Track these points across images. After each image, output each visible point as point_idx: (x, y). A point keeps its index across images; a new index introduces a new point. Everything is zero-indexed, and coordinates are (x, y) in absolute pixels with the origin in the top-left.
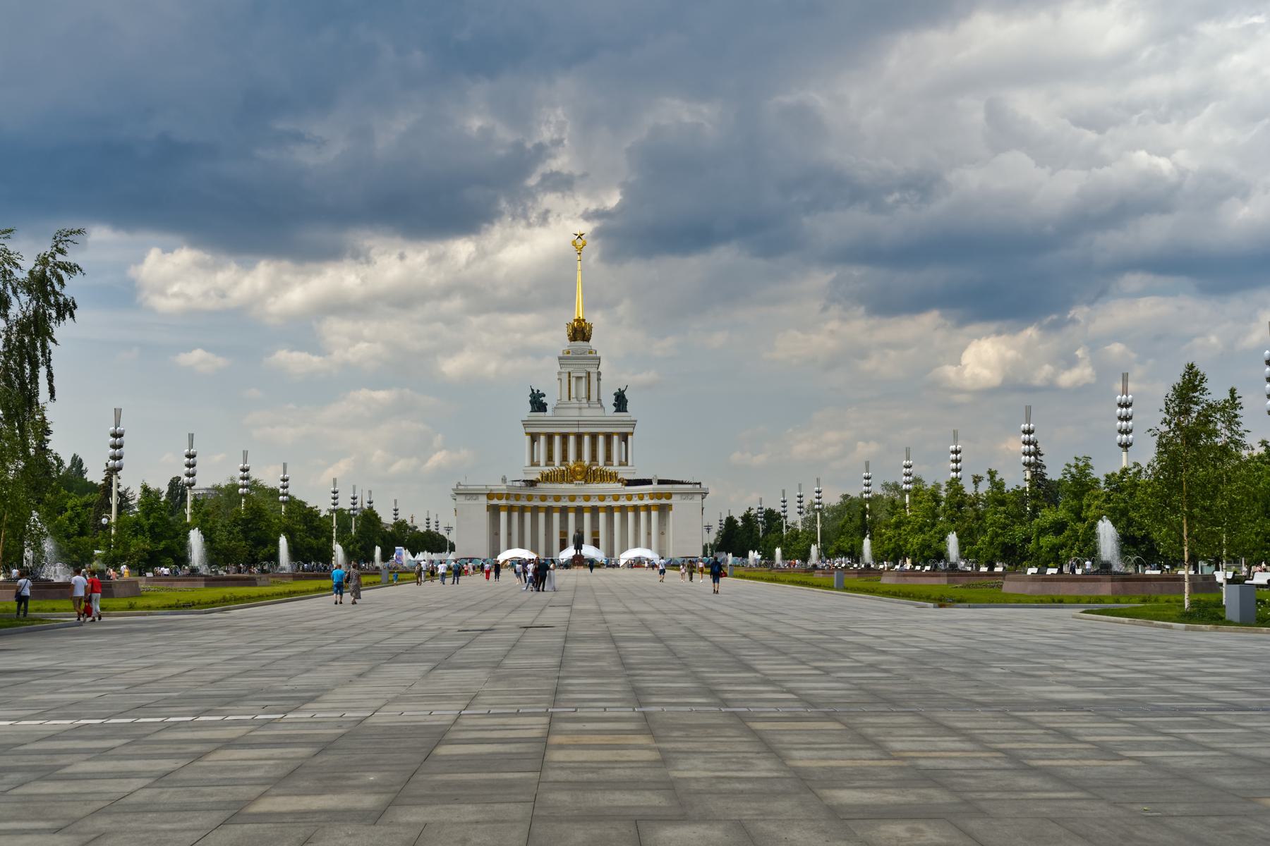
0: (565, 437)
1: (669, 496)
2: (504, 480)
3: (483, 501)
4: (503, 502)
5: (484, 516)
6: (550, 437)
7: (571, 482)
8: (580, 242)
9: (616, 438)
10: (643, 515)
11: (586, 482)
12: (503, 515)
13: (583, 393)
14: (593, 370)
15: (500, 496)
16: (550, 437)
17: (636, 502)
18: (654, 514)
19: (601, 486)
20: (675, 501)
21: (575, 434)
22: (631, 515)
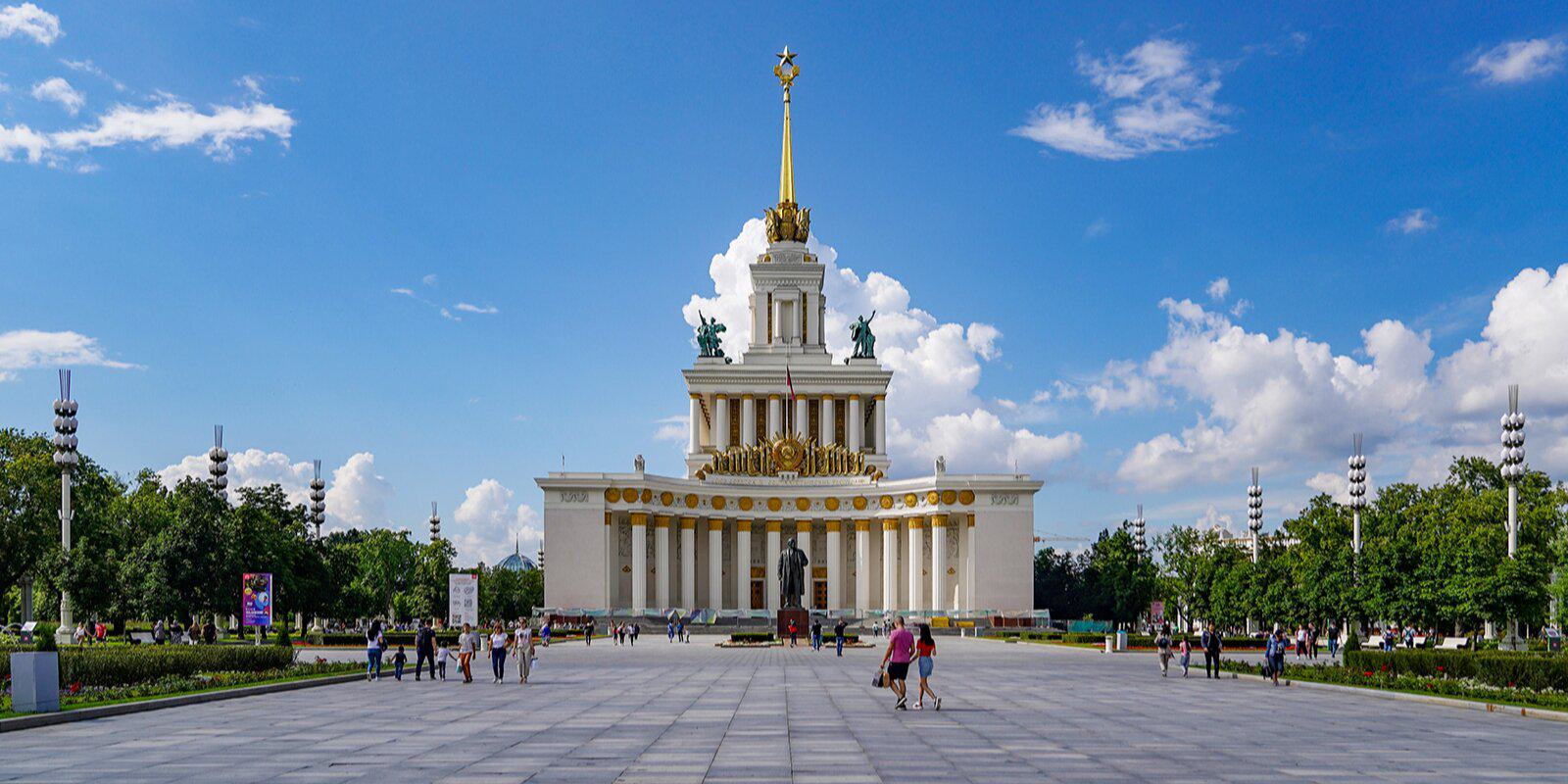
2: (640, 464)
3: (598, 501)
4: (638, 506)
5: (600, 536)
6: (734, 405)
7: (774, 473)
9: (854, 404)
10: (914, 535)
11: (802, 473)
12: (639, 532)
14: (811, 289)
15: (630, 494)
16: (734, 405)
17: (899, 510)
19: (831, 480)
20: (981, 506)
22: (889, 536)
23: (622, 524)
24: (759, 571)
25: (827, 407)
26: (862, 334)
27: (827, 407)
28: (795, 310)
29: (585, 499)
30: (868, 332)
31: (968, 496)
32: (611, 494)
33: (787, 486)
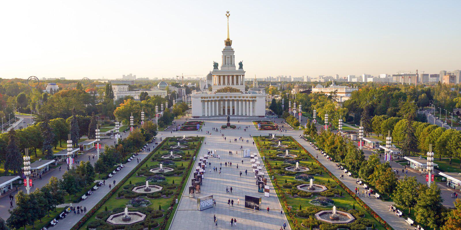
0: (224, 76)
1: (255, 97)
5: (201, 104)
7: (226, 92)
8: (228, 15)
11: (231, 92)
12: (206, 103)
13: (230, 63)
15: (205, 98)
18: (251, 103)
19: (235, 93)
21: (227, 76)
23: (203, 102)
24: (224, 107)
25: (235, 77)
26: (241, 65)
27: (235, 77)
28: (230, 58)
29: (198, 98)
30: (242, 64)
31: (255, 97)
32: (202, 98)
33: (229, 94)
